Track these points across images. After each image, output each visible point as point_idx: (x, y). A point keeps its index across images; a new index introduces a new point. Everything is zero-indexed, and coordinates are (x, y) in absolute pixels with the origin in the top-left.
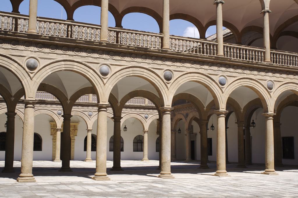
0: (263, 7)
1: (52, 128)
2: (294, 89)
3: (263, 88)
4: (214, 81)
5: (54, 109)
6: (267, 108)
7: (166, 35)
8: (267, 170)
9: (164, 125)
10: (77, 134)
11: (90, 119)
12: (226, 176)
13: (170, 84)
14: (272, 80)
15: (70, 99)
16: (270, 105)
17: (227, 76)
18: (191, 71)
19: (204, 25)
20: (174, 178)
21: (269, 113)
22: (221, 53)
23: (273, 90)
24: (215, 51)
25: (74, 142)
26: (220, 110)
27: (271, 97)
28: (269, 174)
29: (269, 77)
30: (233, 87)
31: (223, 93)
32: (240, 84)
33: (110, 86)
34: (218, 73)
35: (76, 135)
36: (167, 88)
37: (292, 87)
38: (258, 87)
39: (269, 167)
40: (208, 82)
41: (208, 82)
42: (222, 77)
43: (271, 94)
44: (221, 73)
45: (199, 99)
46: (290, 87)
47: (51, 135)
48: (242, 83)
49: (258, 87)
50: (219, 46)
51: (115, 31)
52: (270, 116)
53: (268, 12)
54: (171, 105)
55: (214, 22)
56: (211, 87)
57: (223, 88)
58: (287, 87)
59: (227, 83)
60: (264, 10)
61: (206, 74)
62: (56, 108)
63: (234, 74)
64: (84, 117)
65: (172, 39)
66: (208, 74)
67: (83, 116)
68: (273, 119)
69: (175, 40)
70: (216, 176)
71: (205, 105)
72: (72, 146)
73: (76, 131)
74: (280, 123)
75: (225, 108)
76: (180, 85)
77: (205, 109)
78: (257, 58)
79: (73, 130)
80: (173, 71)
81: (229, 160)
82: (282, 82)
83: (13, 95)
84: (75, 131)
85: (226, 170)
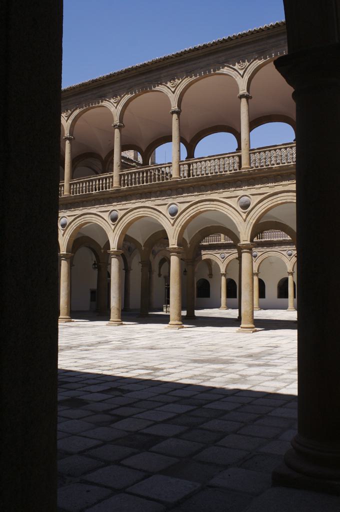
5: (283, 249)
12: (172, 329)
15: (144, 246)
30: (186, 216)
32: (195, 209)
33: (67, 237)
34: (167, 201)
38: (224, 209)
44: (170, 201)
46: (281, 198)
48: (199, 208)
49: (224, 209)
51: (186, 164)
55: (169, 139)
62: (285, 249)
75: (176, 244)
83: (102, 247)
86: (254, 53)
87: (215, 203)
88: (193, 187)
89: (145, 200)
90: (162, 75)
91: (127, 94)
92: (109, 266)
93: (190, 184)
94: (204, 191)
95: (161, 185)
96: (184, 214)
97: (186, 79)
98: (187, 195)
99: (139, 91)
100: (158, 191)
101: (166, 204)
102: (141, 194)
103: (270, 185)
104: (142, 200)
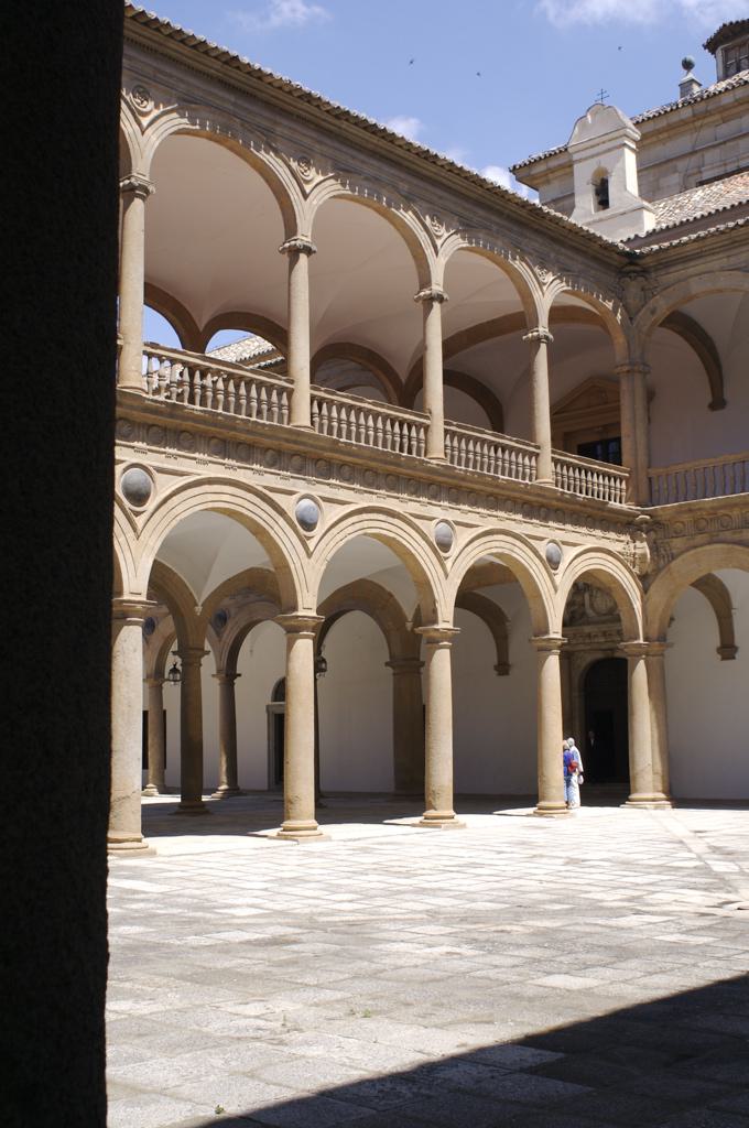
0: (425, 282)
2: (507, 552)
3: (423, 543)
4: (282, 512)
6: (435, 611)
7: (130, 340)
8: (430, 813)
9: (121, 663)
13: (143, 518)
14: (450, 519)
16: (443, 603)
17: (321, 497)
18: (213, 475)
19: (201, 327)
20: (153, 853)
21: (441, 626)
22: (302, 417)
23: (454, 551)
24: (285, 412)
26: (299, 614)
27: (447, 576)
28: (440, 827)
29: (441, 512)
31: (309, 555)
32: (358, 526)
34: (294, 486)
36: (135, 530)
37: (502, 544)
39: (437, 803)
40: (264, 516)
41: (264, 516)
42: (306, 503)
43: (448, 564)
44: (301, 487)
45: (179, 575)
46: (497, 544)
48: (366, 524)
50: (296, 396)
52: (445, 635)
53: (441, 299)
54: (145, 592)
56: (272, 533)
57: (309, 538)
58: (488, 545)
59: (323, 523)
60: (428, 292)
61: (260, 488)
63: (342, 494)
65: (150, 355)
66: (265, 487)
68: (451, 648)
69: (161, 361)
70: (286, 839)
71: (199, 594)
74: (422, 659)
75: (315, 608)
76: (174, 523)
77: (199, 609)
78: (406, 446)
80: (153, 471)
81: (322, 788)
82: (477, 526)
85: (316, 819)
86: (456, 218)
87: (396, 521)
88: (353, 467)
89: (233, 463)
90: (279, 130)
91: (180, 111)
92: (422, 670)
93: (348, 459)
94: (370, 485)
95: (294, 438)
96: (334, 531)
97: (332, 181)
98: (338, 482)
99: (213, 129)
100: (268, 449)
101: (291, 493)
102: (224, 441)
103: (480, 510)
104: (226, 461)
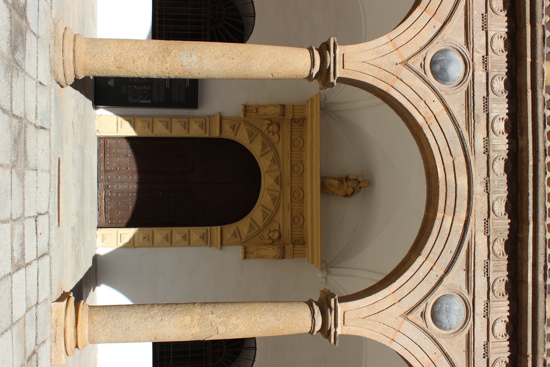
1: (283, 106)
10: (254, 263)
11: (416, 316)
25: (207, 241)
35: (246, 255)
47: (246, 108)
62: (479, 39)
64: (428, 265)
67: (433, 257)
72: (178, 232)
73: (272, 251)
79: (276, 235)
84: (273, 243)
